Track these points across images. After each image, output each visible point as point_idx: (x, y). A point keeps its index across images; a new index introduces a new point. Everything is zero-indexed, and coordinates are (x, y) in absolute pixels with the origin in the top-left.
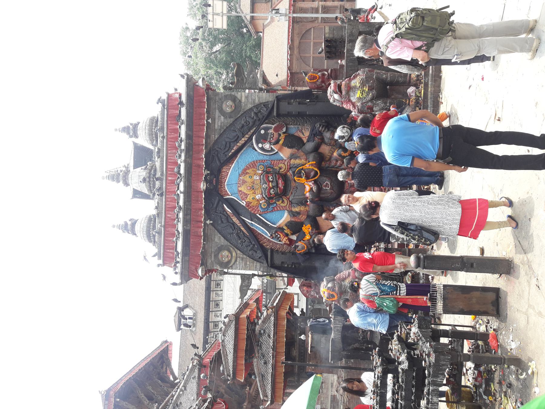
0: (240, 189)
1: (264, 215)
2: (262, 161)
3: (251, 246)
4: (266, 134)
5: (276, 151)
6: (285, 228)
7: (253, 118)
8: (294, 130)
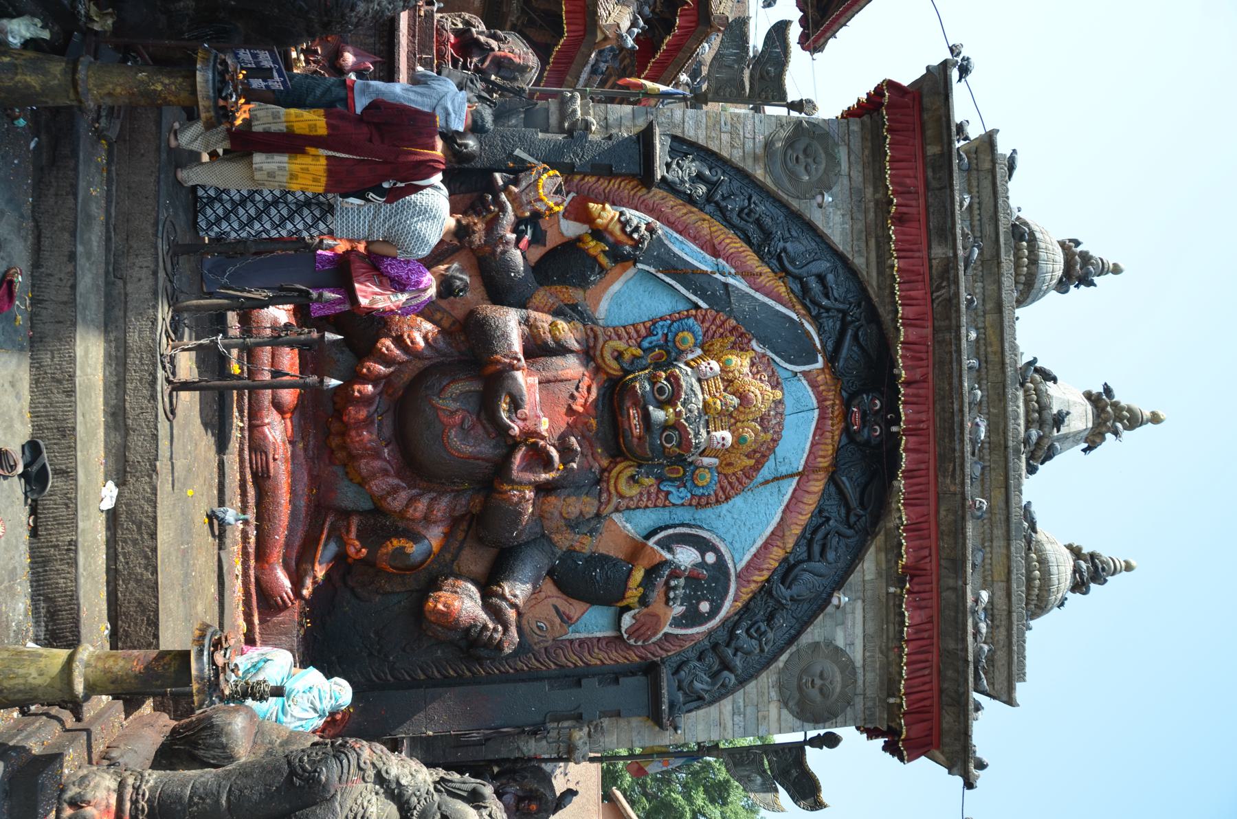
0: (779, 394)
1: (681, 306)
2: (701, 503)
3: (718, 197)
4: (691, 601)
5: (651, 543)
6: (604, 260)
7: (737, 650)
8: (593, 622)
